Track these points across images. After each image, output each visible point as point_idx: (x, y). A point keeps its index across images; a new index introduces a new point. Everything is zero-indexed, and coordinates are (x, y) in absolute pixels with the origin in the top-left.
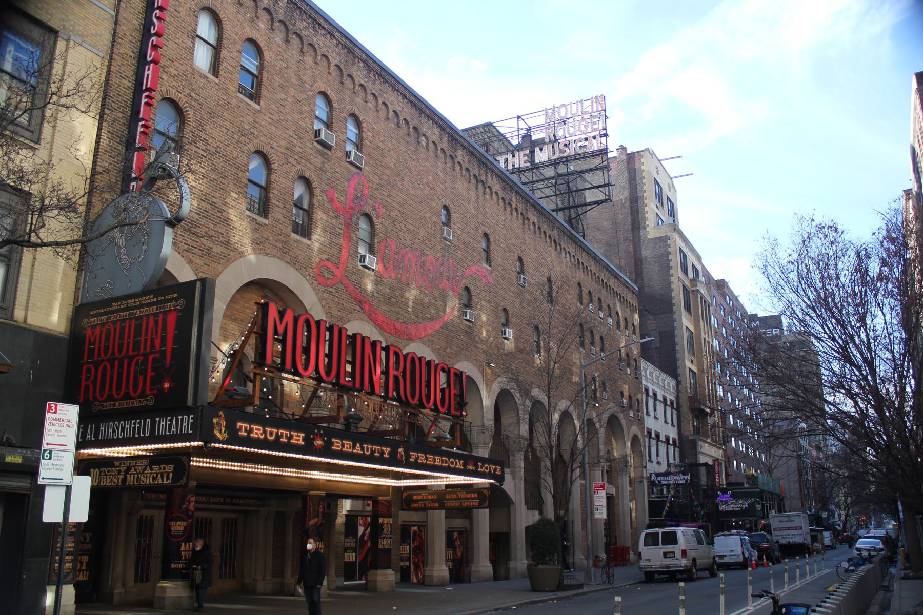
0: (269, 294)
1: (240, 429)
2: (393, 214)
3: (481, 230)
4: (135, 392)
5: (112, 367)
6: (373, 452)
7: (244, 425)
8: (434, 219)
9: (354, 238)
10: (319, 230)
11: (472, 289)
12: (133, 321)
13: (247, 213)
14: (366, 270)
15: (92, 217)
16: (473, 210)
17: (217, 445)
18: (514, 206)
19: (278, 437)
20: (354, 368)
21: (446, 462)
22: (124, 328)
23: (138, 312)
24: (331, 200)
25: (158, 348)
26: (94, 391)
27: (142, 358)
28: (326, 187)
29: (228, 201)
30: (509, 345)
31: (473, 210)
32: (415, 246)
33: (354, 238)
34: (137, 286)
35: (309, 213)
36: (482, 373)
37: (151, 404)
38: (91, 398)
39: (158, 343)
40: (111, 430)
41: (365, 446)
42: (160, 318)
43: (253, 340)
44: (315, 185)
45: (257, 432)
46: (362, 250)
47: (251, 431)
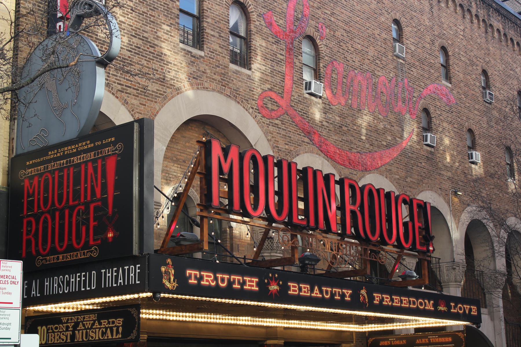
0: (210, 132)
1: (190, 277)
2: (338, 34)
3: (438, 43)
4: (78, 244)
5: (53, 219)
6: (333, 295)
7: (193, 272)
8: (384, 35)
9: (298, 64)
10: (259, 58)
11: (431, 110)
12: (71, 169)
13: (181, 45)
14: (313, 98)
15: (21, 63)
16: (427, 23)
17: (167, 295)
18: (474, 12)
19: (230, 283)
20: (306, 205)
21: (414, 303)
22: (61, 177)
23: (76, 160)
24: (270, 25)
25: (98, 195)
26: (37, 245)
27: (83, 207)
28: (264, 11)
29: (159, 34)
30: (478, 170)
31: (427, 23)
32: (365, 67)
33: (298, 64)
34: (72, 133)
35: (247, 41)
36: (448, 203)
37: (95, 255)
38: (34, 253)
39: (98, 191)
40: (56, 285)
41: (324, 289)
42: (99, 164)
43: (197, 182)
44: (251, 9)
45: (208, 279)
46: (307, 76)
47: (201, 278)
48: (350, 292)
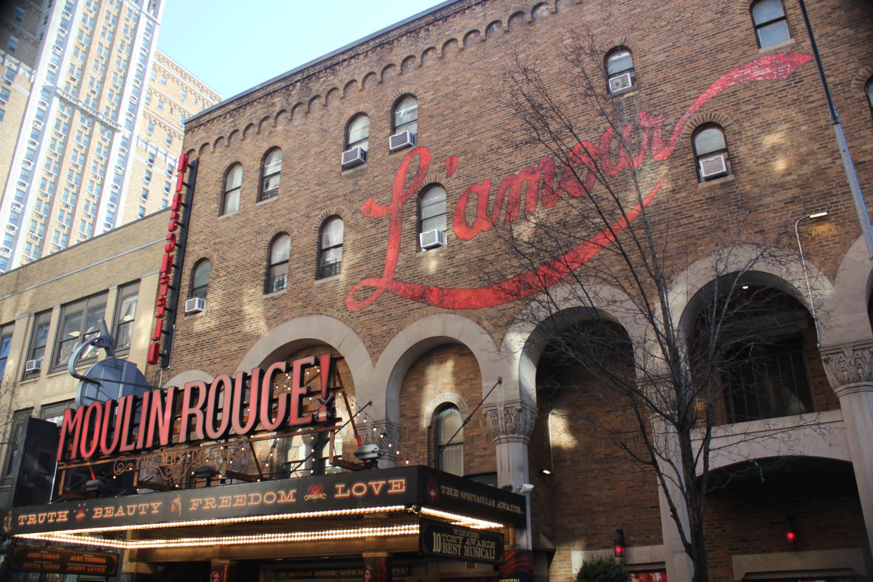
41: (129, 507)
48: (159, 504)
